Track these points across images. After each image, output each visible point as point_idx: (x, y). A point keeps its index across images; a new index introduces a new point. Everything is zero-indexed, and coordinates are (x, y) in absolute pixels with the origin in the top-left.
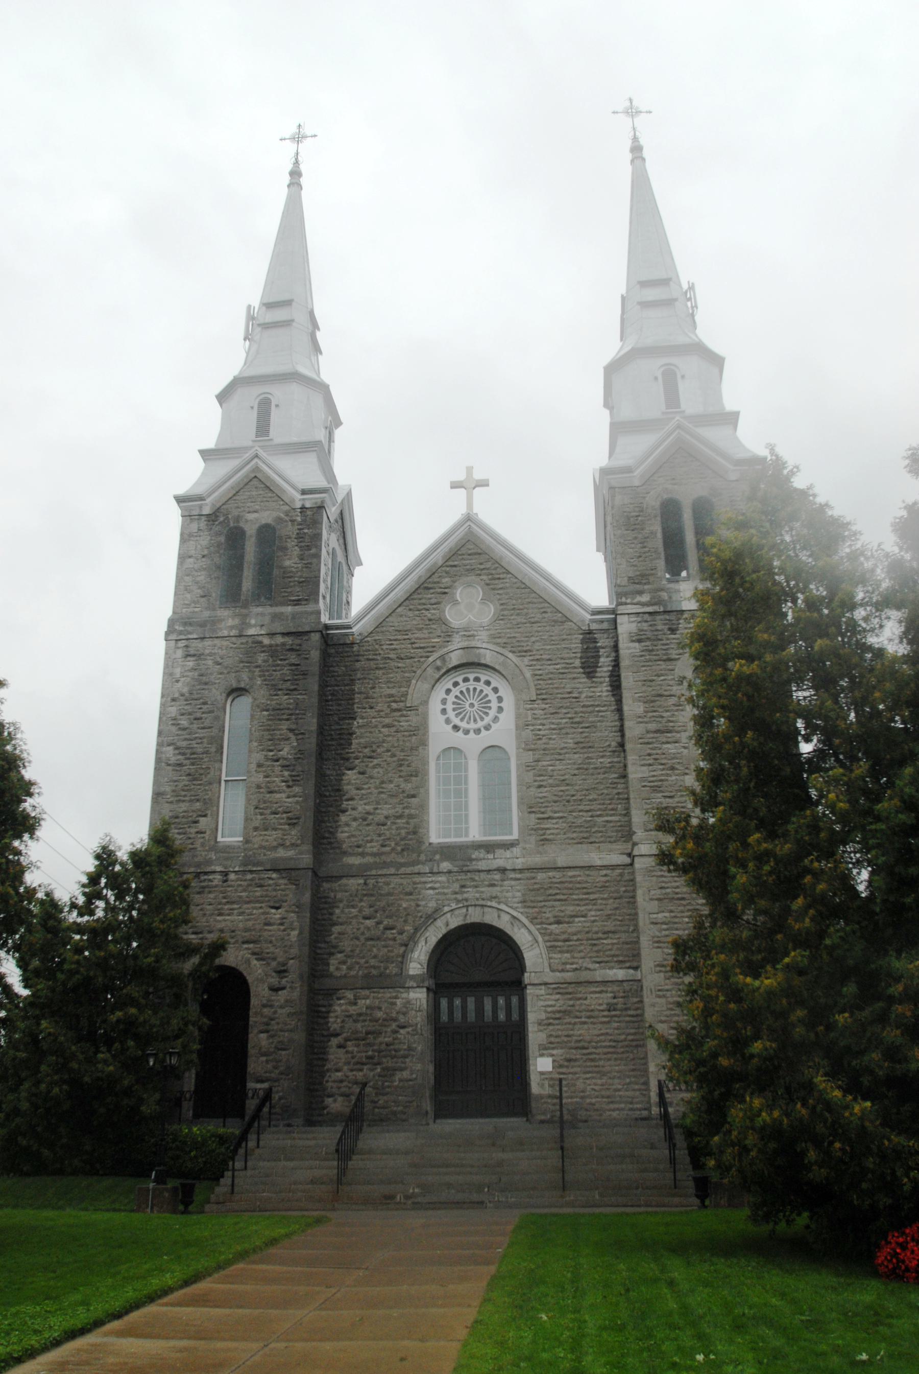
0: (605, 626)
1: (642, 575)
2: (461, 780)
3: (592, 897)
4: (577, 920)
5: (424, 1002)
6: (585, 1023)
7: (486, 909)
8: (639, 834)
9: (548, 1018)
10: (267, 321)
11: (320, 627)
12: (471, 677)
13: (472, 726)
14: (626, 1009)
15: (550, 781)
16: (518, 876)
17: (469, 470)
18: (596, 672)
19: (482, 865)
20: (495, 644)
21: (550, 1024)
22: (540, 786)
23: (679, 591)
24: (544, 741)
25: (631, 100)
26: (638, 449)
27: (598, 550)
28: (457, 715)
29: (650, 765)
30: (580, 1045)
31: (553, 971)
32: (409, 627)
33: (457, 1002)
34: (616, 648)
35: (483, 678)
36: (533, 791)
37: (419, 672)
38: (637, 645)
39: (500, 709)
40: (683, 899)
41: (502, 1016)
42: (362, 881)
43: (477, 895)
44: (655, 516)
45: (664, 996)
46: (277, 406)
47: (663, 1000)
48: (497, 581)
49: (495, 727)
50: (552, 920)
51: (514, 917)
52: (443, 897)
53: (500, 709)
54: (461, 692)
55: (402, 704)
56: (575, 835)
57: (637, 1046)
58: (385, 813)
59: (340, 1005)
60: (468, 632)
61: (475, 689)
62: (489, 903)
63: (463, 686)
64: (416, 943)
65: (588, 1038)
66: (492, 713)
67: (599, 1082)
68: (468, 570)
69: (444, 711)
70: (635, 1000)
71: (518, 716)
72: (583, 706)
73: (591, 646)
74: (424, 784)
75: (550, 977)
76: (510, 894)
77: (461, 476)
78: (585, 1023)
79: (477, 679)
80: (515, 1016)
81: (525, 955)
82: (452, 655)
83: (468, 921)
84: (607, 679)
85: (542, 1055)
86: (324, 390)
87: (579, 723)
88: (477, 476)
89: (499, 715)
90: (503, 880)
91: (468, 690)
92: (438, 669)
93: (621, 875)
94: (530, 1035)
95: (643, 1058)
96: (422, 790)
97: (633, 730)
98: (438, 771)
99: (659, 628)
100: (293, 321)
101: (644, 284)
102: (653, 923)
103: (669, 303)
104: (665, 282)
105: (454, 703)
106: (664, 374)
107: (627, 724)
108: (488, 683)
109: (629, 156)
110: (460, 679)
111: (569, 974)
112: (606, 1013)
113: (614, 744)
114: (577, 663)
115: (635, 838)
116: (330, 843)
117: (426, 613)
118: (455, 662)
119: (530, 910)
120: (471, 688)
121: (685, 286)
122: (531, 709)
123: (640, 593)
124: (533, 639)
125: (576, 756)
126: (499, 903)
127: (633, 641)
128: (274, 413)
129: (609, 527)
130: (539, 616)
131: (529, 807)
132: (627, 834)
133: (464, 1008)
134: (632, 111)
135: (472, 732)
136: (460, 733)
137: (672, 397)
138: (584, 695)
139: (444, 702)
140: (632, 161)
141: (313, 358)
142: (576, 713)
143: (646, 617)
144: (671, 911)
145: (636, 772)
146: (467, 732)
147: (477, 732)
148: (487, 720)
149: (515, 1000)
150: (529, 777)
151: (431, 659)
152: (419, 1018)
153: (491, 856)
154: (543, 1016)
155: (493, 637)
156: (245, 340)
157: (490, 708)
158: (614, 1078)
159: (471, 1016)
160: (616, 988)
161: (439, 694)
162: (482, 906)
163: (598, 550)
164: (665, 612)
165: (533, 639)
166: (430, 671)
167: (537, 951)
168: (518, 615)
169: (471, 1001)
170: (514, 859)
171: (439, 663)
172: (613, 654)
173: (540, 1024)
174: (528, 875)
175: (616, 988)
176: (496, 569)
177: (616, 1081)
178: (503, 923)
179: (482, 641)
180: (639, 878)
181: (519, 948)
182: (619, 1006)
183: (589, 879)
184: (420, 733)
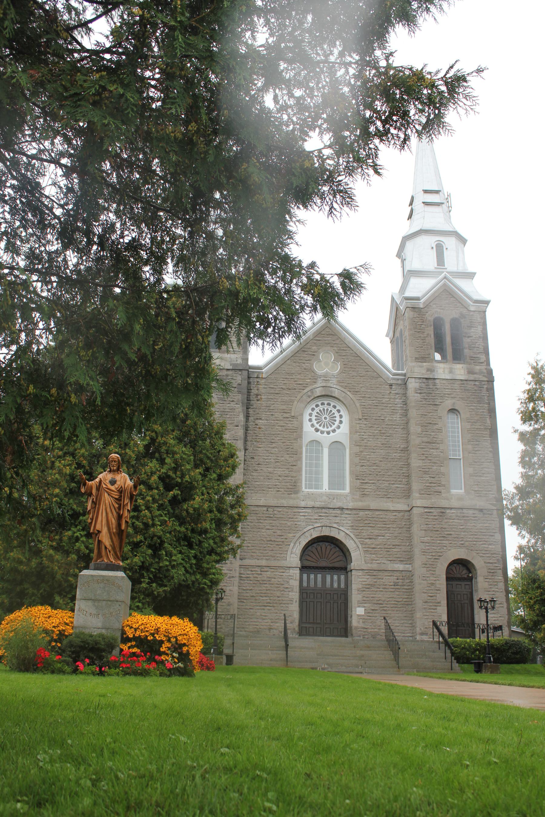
0: (399, 382)
1: (423, 358)
2: (319, 458)
3: (388, 526)
5: (298, 575)
7: (332, 529)
8: (416, 495)
11: (247, 368)
13: (325, 429)
16: (350, 512)
22: (362, 466)
27: (387, 335)
28: (317, 423)
30: (380, 602)
32: (293, 372)
33: (312, 576)
34: (405, 395)
35: (332, 404)
36: (358, 468)
39: (341, 422)
41: (335, 585)
42: (265, 509)
44: (431, 326)
47: (425, 582)
49: (338, 431)
50: (367, 537)
52: (309, 520)
54: (320, 410)
56: (380, 493)
57: (407, 605)
58: (279, 472)
59: (253, 574)
60: (326, 378)
61: (327, 409)
63: (321, 407)
64: (295, 543)
65: (383, 599)
66: (337, 423)
69: (310, 420)
71: (351, 427)
74: (300, 459)
76: (345, 522)
79: (329, 404)
80: (343, 586)
81: (353, 554)
82: (317, 390)
85: (359, 607)
91: (324, 409)
92: (309, 397)
93: (403, 516)
94: (353, 596)
96: (299, 462)
97: (415, 440)
98: (306, 452)
99: (431, 387)
101: (426, 192)
104: (437, 192)
105: (316, 416)
106: (437, 245)
107: (412, 437)
108: (335, 407)
110: (319, 403)
116: (248, 487)
118: (319, 394)
119: (355, 531)
121: (446, 197)
124: (361, 385)
125: (382, 451)
129: (400, 327)
131: (356, 476)
132: (407, 494)
133: (317, 580)
139: (310, 415)
143: (424, 380)
145: (415, 462)
146: (322, 432)
147: (328, 433)
148: (334, 427)
149: (343, 577)
150: (357, 460)
151: (305, 391)
152: (295, 584)
154: (361, 586)
155: (339, 382)
157: (335, 421)
158: (395, 620)
159: (319, 585)
160: (399, 575)
163: (387, 335)
165: (361, 385)
166: (304, 397)
167: (358, 552)
169: (319, 576)
171: (309, 393)
174: (354, 512)
175: (398, 574)
177: (396, 622)
178: (340, 537)
179: (333, 383)
180: (415, 519)
181: (348, 550)
182: (400, 584)
183: (387, 517)
184: (298, 431)
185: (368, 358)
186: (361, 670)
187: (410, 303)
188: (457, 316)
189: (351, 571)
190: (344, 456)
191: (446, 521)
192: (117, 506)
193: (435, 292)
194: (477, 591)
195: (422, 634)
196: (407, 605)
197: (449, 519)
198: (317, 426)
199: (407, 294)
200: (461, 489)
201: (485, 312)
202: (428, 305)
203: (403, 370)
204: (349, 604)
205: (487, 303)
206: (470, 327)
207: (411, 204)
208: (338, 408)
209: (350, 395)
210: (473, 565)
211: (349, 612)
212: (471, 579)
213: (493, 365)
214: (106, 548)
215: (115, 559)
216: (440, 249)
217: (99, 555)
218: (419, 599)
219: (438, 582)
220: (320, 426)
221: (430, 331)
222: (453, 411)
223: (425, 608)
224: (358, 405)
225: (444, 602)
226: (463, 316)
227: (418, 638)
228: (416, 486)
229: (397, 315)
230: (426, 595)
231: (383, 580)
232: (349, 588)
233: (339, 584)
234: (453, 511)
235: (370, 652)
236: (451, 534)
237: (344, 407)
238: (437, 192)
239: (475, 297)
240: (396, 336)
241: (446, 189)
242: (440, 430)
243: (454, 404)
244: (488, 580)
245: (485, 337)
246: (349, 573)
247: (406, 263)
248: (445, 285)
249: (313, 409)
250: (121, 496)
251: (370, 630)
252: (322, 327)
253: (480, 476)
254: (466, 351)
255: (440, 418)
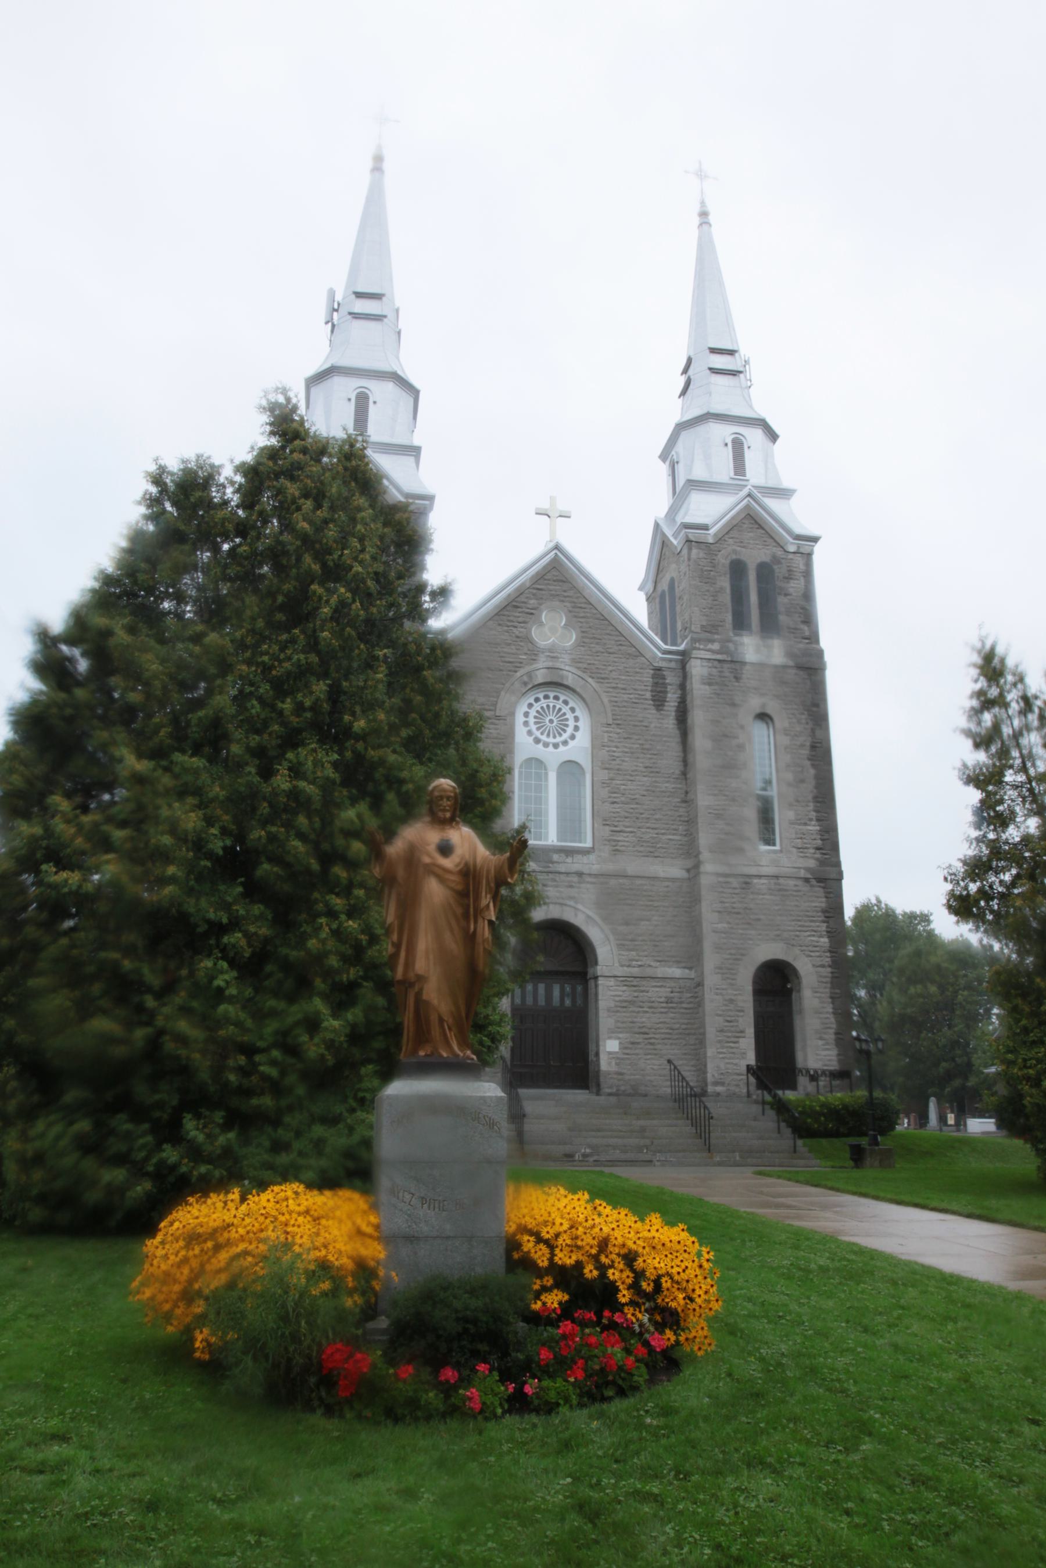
0: (673, 665)
2: (541, 789)
3: (656, 904)
4: (643, 923)
6: (647, 1012)
8: (705, 855)
9: (616, 1006)
10: (356, 311)
12: (552, 695)
13: (551, 740)
14: (681, 1003)
15: (623, 799)
17: (552, 499)
18: (663, 705)
19: (562, 868)
20: (578, 668)
21: (618, 1011)
22: (614, 803)
23: (742, 644)
24: (618, 761)
25: (700, 163)
26: (710, 510)
27: (641, 589)
28: (538, 729)
29: (715, 795)
30: (643, 1030)
31: (622, 966)
34: (683, 687)
37: (507, 685)
38: (707, 687)
39: (576, 728)
40: (738, 913)
43: (558, 894)
45: (721, 994)
46: (375, 402)
48: (577, 610)
49: (572, 743)
51: (589, 917)
53: (576, 728)
54: (542, 708)
55: (492, 713)
56: (642, 849)
57: (689, 1034)
60: (552, 653)
61: (554, 707)
62: (569, 902)
63: (543, 703)
66: (570, 730)
67: (657, 1062)
68: (552, 595)
69: (526, 724)
70: (689, 995)
71: (594, 738)
72: (654, 735)
73: (661, 681)
75: (620, 971)
77: (545, 505)
78: (647, 1012)
79: (556, 698)
80: (579, 1002)
83: (550, 916)
84: (673, 714)
85: (610, 1038)
86: (414, 392)
87: (648, 750)
88: (562, 506)
89: (576, 734)
90: (580, 883)
91: (548, 706)
92: (525, 684)
95: (695, 1044)
99: (727, 674)
100: (385, 316)
101: (713, 351)
102: (714, 932)
103: (734, 373)
104: (731, 353)
105: (535, 717)
108: (566, 703)
109: (696, 220)
110: (541, 696)
111: (636, 969)
112: (664, 1005)
113: (677, 772)
114: (648, 695)
115: (702, 857)
117: (515, 630)
118: (540, 680)
120: (551, 705)
122: (607, 732)
123: (712, 641)
124: (610, 668)
126: (576, 903)
127: (704, 684)
128: (372, 410)
130: (616, 648)
132: (690, 850)
134: (701, 175)
135: (551, 746)
136: (540, 746)
137: (739, 466)
138: (653, 725)
139: (526, 714)
140: (701, 224)
141: (398, 358)
142: (646, 740)
144: (729, 923)
145: (704, 800)
146: (546, 745)
147: (556, 746)
148: (565, 736)
149: (579, 988)
150: (604, 793)
151: (518, 674)
153: (569, 860)
154: (612, 1004)
155: (574, 661)
156: (327, 323)
157: (567, 726)
159: (542, 1001)
160: (673, 985)
161: (522, 708)
162: (561, 904)
163: (641, 589)
164: (732, 661)
165: (610, 668)
168: (597, 644)
169: (541, 987)
170: (591, 864)
171: (525, 678)
172: (679, 692)
173: (609, 1010)
176: (577, 598)
178: (578, 920)
180: (703, 892)
182: (676, 1000)
185: (622, 622)
186: (648, 1157)
187: (693, 534)
188: (767, 559)
189: (596, 978)
190: (580, 784)
191: (751, 897)
192: (459, 911)
193: (733, 518)
194: (801, 1011)
195: (716, 1083)
196: (689, 1034)
197: (758, 894)
198: (538, 734)
199: (689, 519)
200: (774, 844)
201: (809, 556)
202: (720, 539)
203: (674, 644)
204: (592, 1034)
205: (815, 540)
206: (788, 578)
207: (685, 371)
208: (571, 704)
209: (594, 684)
210: (794, 971)
211: (592, 1047)
212: (790, 991)
213: (826, 641)
214: (441, 1020)
215: (460, 1045)
216: (738, 447)
217: (422, 1036)
218: (712, 1025)
219: (740, 998)
220: (542, 734)
221: (725, 583)
222: (763, 717)
223: (720, 1042)
224: (606, 700)
225: (750, 1031)
226: (776, 560)
227: (710, 1089)
228: (704, 839)
229: (662, 551)
230: (721, 1019)
231: (649, 994)
232: (592, 1006)
233: (574, 1001)
234: (763, 881)
235: (655, 1122)
236: (759, 920)
237: (581, 704)
238: (731, 353)
239: (798, 530)
240: (659, 589)
241: (744, 351)
242: (741, 747)
243: (764, 705)
244: (818, 995)
245: (808, 596)
246: (592, 983)
247: (680, 469)
248: (748, 507)
249: (530, 706)
250: (467, 885)
251: (627, 1077)
252: (544, 567)
253: (805, 824)
254: (783, 618)
255: (742, 727)
